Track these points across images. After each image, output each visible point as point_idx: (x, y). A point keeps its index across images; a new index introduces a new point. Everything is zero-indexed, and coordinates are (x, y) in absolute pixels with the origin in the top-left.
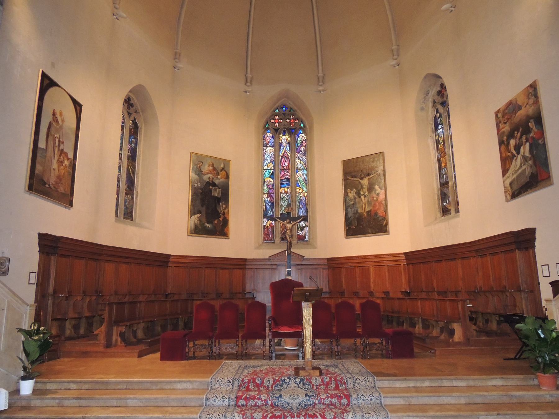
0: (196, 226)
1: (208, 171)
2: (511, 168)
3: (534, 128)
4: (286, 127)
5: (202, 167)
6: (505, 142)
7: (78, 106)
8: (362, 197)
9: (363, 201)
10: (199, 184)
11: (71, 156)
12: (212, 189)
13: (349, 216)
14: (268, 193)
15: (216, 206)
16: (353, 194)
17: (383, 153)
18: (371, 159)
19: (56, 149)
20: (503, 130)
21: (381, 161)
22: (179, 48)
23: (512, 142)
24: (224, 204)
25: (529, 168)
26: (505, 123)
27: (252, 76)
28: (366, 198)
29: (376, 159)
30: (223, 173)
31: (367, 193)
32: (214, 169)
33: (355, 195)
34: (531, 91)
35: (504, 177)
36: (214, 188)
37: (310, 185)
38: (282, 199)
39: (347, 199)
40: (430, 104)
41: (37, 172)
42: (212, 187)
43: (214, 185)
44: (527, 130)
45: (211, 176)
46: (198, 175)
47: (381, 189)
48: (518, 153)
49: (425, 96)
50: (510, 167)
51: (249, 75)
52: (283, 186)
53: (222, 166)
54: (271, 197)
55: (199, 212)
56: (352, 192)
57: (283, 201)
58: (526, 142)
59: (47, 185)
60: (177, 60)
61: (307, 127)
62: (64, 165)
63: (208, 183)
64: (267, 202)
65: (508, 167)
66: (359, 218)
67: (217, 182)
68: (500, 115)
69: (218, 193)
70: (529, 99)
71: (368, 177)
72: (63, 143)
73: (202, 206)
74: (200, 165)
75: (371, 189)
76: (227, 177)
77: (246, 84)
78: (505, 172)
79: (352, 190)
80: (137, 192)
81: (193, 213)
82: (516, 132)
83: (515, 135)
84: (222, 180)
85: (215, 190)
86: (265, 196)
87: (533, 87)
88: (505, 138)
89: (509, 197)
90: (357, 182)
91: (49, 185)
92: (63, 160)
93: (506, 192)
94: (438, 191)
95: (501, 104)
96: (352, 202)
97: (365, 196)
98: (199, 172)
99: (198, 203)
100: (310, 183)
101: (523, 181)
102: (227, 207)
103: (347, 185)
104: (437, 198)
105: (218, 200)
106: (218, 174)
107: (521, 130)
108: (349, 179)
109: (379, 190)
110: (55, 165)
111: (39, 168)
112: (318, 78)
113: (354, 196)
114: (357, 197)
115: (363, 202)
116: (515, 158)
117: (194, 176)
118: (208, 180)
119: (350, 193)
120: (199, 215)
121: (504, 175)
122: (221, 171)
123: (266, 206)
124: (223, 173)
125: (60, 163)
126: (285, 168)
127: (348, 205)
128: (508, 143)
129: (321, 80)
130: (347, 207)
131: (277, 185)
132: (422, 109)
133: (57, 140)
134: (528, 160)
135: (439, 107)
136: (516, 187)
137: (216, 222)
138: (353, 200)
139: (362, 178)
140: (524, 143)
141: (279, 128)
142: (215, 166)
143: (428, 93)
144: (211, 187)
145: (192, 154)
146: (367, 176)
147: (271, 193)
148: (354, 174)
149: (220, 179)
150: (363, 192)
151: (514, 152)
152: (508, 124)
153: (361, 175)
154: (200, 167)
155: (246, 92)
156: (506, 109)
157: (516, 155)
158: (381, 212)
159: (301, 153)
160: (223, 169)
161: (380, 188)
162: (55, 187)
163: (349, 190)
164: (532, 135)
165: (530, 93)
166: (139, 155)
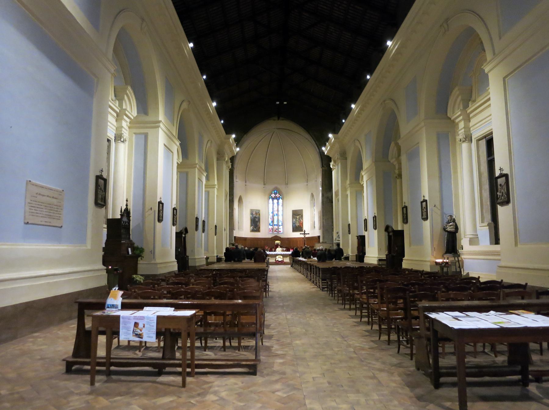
0: (252, 229)
13: (294, 226)
43: (256, 217)
45: (255, 215)
51: (265, 183)
55: (253, 225)
66: (296, 227)
67: (257, 216)
76: (260, 215)
87: (500, 38)
98: (252, 214)
99: (252, 223)
105: (257, 222)
106: (257, 214)
109: (301, 220)
117: (251, 216)
124: (258, 214)
129: (287, 184)
130: (293, 224)
137: (257, 228)
158: (301, 226)
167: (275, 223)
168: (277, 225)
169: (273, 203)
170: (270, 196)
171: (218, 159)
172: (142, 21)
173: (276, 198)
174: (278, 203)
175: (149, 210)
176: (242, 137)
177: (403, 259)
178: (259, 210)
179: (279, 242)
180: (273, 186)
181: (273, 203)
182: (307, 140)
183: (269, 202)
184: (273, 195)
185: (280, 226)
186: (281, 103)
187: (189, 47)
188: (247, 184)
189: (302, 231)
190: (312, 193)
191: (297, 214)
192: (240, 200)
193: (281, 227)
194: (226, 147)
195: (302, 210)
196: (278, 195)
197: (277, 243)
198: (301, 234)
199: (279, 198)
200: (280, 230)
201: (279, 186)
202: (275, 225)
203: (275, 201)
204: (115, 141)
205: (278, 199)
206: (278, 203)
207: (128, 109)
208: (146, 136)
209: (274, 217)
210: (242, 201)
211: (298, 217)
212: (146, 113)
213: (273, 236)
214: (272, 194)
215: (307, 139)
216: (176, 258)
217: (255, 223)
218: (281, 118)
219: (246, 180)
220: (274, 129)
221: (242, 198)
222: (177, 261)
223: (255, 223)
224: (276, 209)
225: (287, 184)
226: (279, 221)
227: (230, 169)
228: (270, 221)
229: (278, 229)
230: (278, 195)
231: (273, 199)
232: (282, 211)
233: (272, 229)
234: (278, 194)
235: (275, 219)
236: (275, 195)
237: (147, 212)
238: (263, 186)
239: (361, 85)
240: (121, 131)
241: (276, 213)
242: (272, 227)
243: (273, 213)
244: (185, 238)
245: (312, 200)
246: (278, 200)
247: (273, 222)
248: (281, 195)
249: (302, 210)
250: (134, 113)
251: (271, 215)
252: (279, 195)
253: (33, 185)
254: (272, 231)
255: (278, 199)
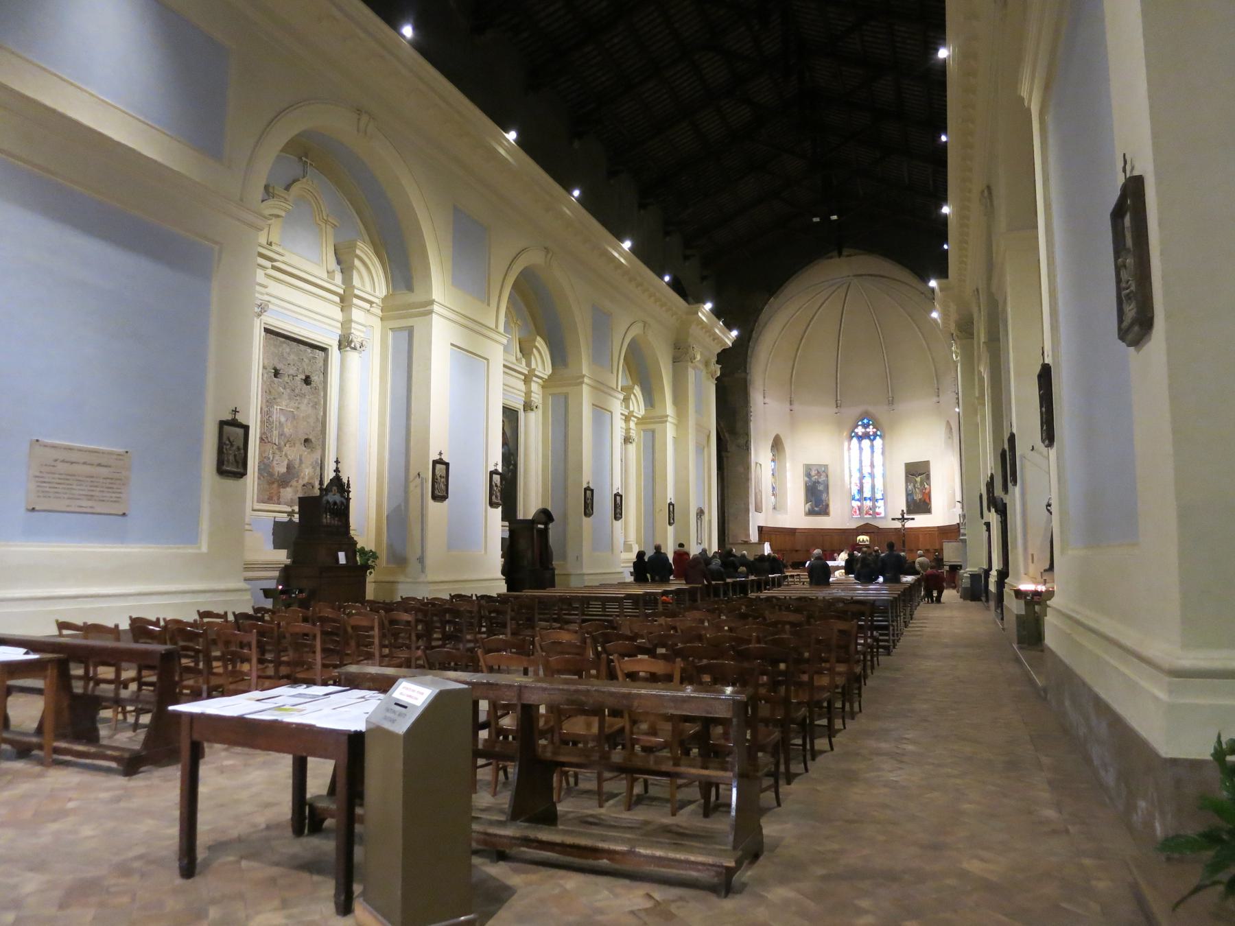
0: (809, 510)
13: (909, 500)
32: (818, 472)
43: (818, 482)
46: (809, 478)
51: (839, 402)
53: (823, 469)
67: (820, 480)
76: (827, 476)
81: (807, 501)
98: (808, 475)
103: (907, 480)
106: (821, 475)
109: (926, 486)
117: (807, 479)
120: (810, 503)
129: (891, 402)
130: (908, 494)
137: (821, 506)
158: (928, 501)
167: (867, 494)
168: (870, 499)
169: (861, 449)
170: (853, 431)
171: (676, 360)
172: (359, 114)
173: (866, 436)
174: (872, 447)
175: (415, 477)
176: (766, 304)
177: (1006, 581)
179: (865, 539)
180: (858, 410)
181: (861, 449)
182: (923, 296)
183: (852, 446)
184: (860, 430)
185: (877, 500)
186: (826, 219)
187: (507, 141)
188: (796, 407)
189: (909, 512)
190: (948, 422)
191: (917, 473)
192: (777, 445)
193: (880, 503)
194: (695, 330)
195: (927, 464)
196: (871, 430)
197: (861, 540)
199: (875, 435)
200: (877, 510)
201: (871, 409)
202: (865, 499)
203: (866, 443)
204: (340, 349)
205: (872, 437)
206: (872, 447)
207: (368, 288)
208: (410, 330)
209: (864, 481)
211: (918, 479)
212: (410, 288)
213: (862, 523)
214: (857, 426)
215: (922, 293)
216: (503, 573)
217: (817, 497)
218: (845, 252)
219: (791, 398)
220: (849, 276)
221: (784, 442)
222: (504, 578)
223: (817, 497)
224: (867, 462)
225: (892, 404)
226: (876, 490)
227: (717, 379)
228: (855, 490)
229: (874, 507)
230: (871, 430)
231: (860, 438)
232: (883, 465)
233: (859, 509)
234: (871, 427)
235: (864, 485)
236: (866, 428)
237: (414, 479)
238: (836, 410)
239: (939, 157)
240: (350, 328)
241: (867, 470)
242: (859, 504)
243: (860, 470)
244: (546, 530)
245: (949, 438)
246: (872, 441)
247: (861, 491)
248: (878, 430)
249: (927, 464)
250: (381, 289)
251: (856, 475)
252: (875, 430)
253: (45, 446)
254: (860, 514)
255: (872, 437)
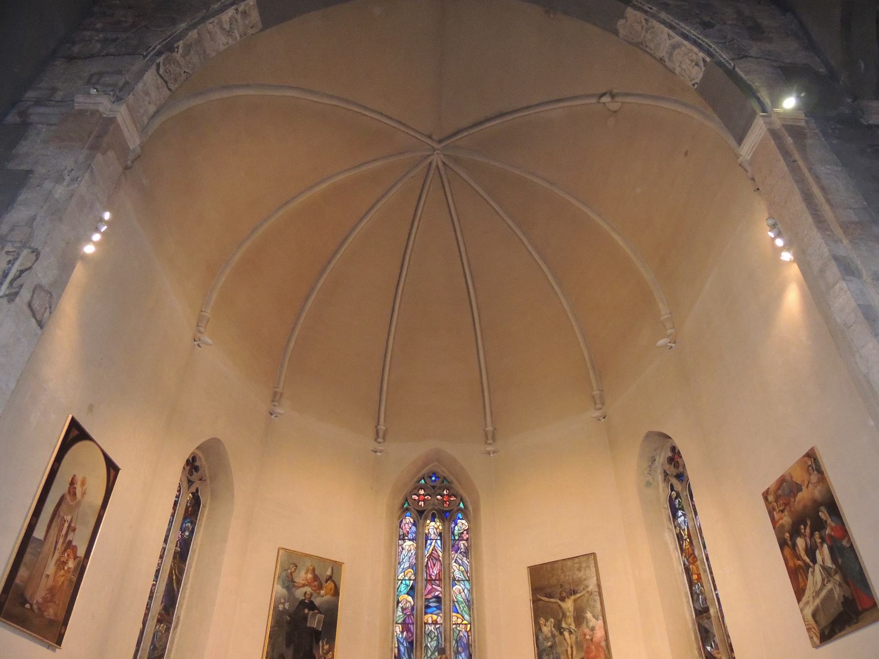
1: (304, 582)
2: (808, 587)
3: (829, 521)
4: (436, 508)
5: (295, 575)
6: (790, 543)
7: (112, 469)
8: (566, 634)
9: (568, 640)
10: (287, 606)
11: (81, 553)
12: (308, 614)
14: (404, 623)
15: (311, 648)
16: (550, 628)
17: (594, 554)
18: (576, 565)
19: (61, 541)
20: (781, 522)
21: (593, 570)
22: (281, 386)
23: (800, 542)
24: (326, 644)
25: (838, 588)
26: (782, 511)
27: (386, 429)
28: (572, 636)
29: (584, 565)
30: (330, 585)
31: (573, 627)
32: (316, 578)
33: (553, 629)
34: (810, 463)
35: (801, 603)
36: (311, 612)
37: (475, 610)
38: (428, 635)
39: (540, 637)
40: (660, 478)
41: (17, 581)
42: (309, 610)
43: (312, 606)
44: (819, 525)
46: (288, 588)
47: (597, 619)
48: (814, 561)
49: (650, 464)
50: (805, 585)
51: (382, 427)
52: (429, 610)
53: (329, 573)
54: (409, 630)
56: (548, 624)
57: (430, 640)
58: (822, 543)
59: (28, 606)
60: (276, 404)
61: (470, 508)
62: (66, 568)
63: (302, 603)
64: (402, 641)
65: (802, 585)
67: (317, 601)
68: (771, 498)
69: (319, 622)
70: (810, 474)
71: (573, 597)
72: (74, 530)
73: (288, 646)
74: (293, 570)
75: (579, 619)
76: (336, 592)
77: (376, 440)
78: (799, 593)
79: (547, 620)
80: (178, 618)
82: (802, 527)
83: (803, 531)
84: (328, 597)
85: (314, 615)
86: (398, 629)
88: (787, 535)
89: (817, 640)
90: (555, 606)
91: (31, 605)
92: (67, 560)
93: (809, 630)
94: (694, 624)
95: (770, 481)
96: (549, 644)
97: (570, 633)
98: (289, 583)
99: (282, 640)
100: (475, 605)
101: (835, 609)
102: (332, 649)
103: (540, 611)
104: (693, 638)
105: (316, 635)
106: (320, 587)
107: (809, 523)
108: (542, 600)
109: (593, 622)
110: (51, 569)
111: (23, 572)
112: (486, 436)
113: (551, 632)
114: (557, 633)
115: (568, 643)
116: (811, 569)
117: (280, 589)
118: (304, 598)
119: (545, 625)
121: (799, 600)
122: (326, 583)
123: (398, 647)
124: (330, 585)
125: (61, 564)
126: (433, 578)
127: (542, 648)
128: (794, 545)
129: (490, 437)
131: (418, 609)
132: (648, 484)
133: (66, 525)
134: (832, 575)
135: (675, 481)
136: (824, 622)
138: (549, 638)
139: (563, 599)
140: (819, 545)
141: (425, 509)
142: (316, 572)
143: (655, 460)
144: (306, 611)
145: (281, 551)
146: (571, 595)
147: (409, 623)
148: (548, 590)
149: (323, 596)
150: (566, 624)
151: (808, 560)
152: (786, 513)
153: (561, 593)
154: (291, 573)
155: (376, 452)
156: (779, 489)
157: (811, 564)
159: (460, 553)
160: (330, 578)
161: (594, 616)
162: (39, 609)
163: (542, 621)
164: (828, 531)
165: (810, 466)
166: (194, 551)
178: (337, 566)
198: (807, 487)
201: (450, 449)
210: (233, 496)
238: (372, 445)
